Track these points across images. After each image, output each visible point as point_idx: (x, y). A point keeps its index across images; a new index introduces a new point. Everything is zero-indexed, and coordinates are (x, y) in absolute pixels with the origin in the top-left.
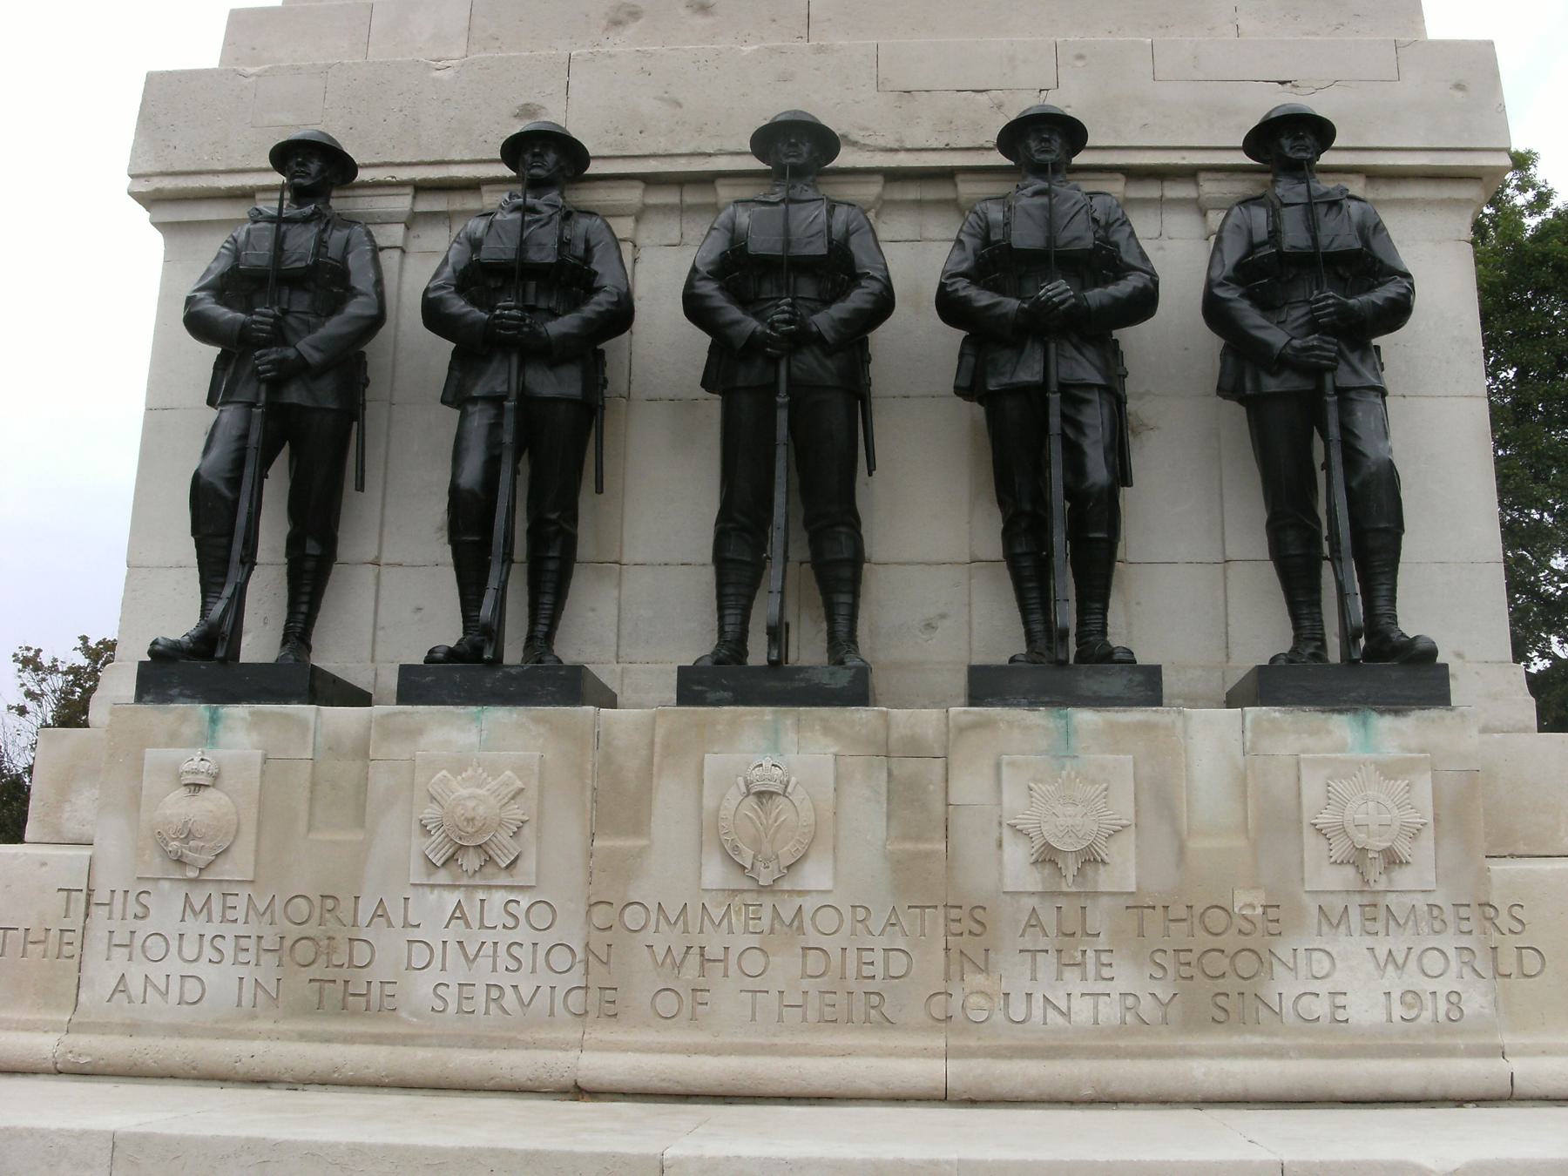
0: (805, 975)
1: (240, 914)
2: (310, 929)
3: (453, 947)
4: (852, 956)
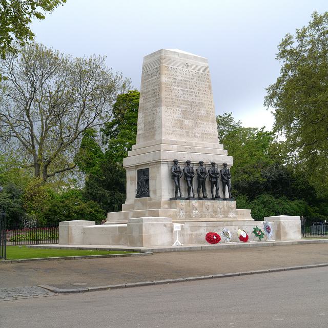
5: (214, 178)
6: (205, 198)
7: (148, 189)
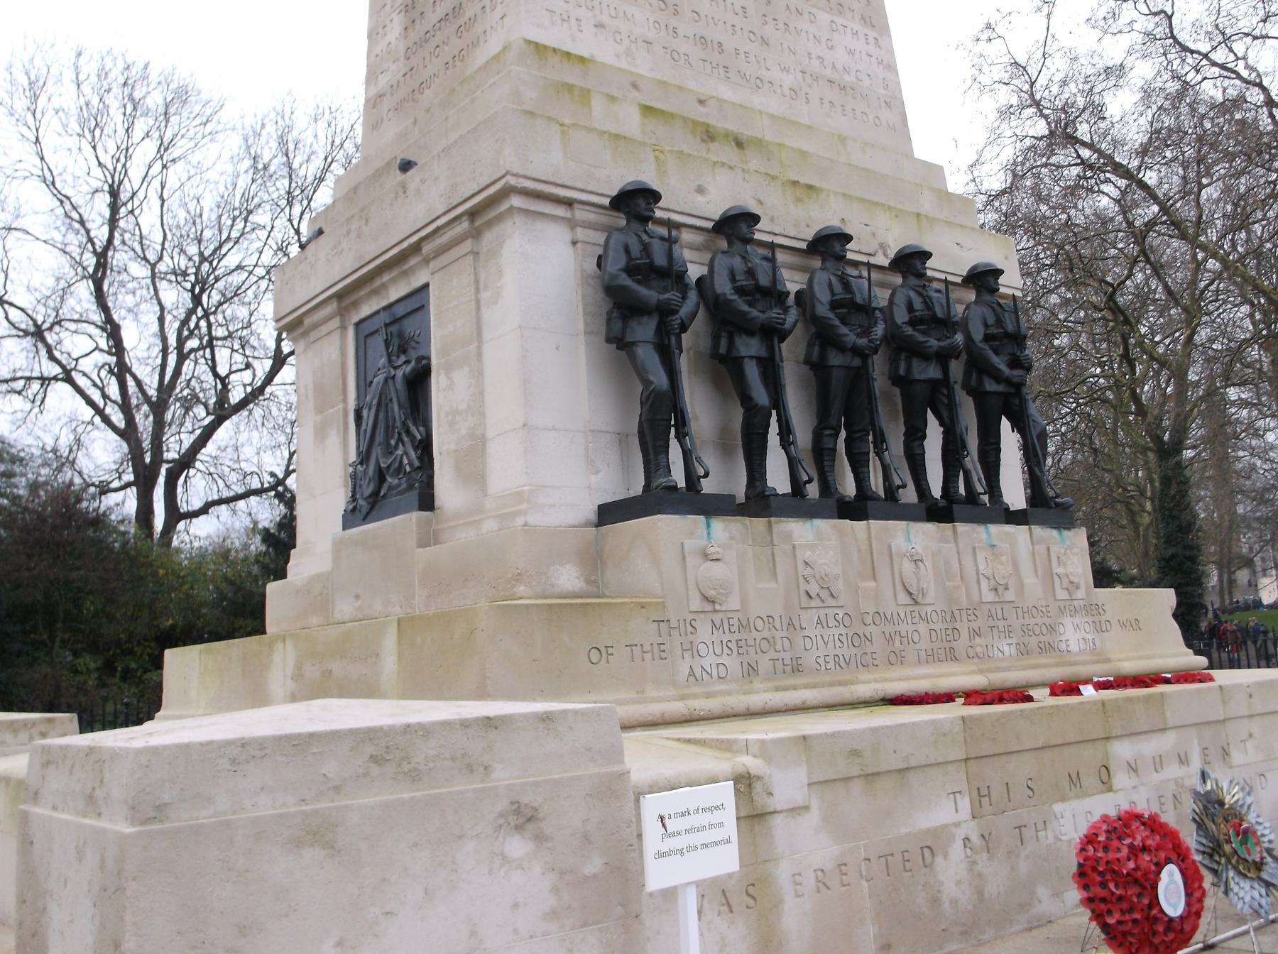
1: (735, 628)
2: (766, 634)
5: (924, 355)
6: (890, 507)
7: (425, 447)
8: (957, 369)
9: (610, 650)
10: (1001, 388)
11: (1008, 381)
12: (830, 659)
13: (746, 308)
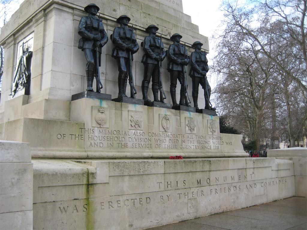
0: (169, 143)
3: (134, 138)
4: (173, 140)
8: (187, 68)
9: (64, 135)
10: (199, 76)
11: (201, 74)
12: (137, 145)
13: (122, 43)
